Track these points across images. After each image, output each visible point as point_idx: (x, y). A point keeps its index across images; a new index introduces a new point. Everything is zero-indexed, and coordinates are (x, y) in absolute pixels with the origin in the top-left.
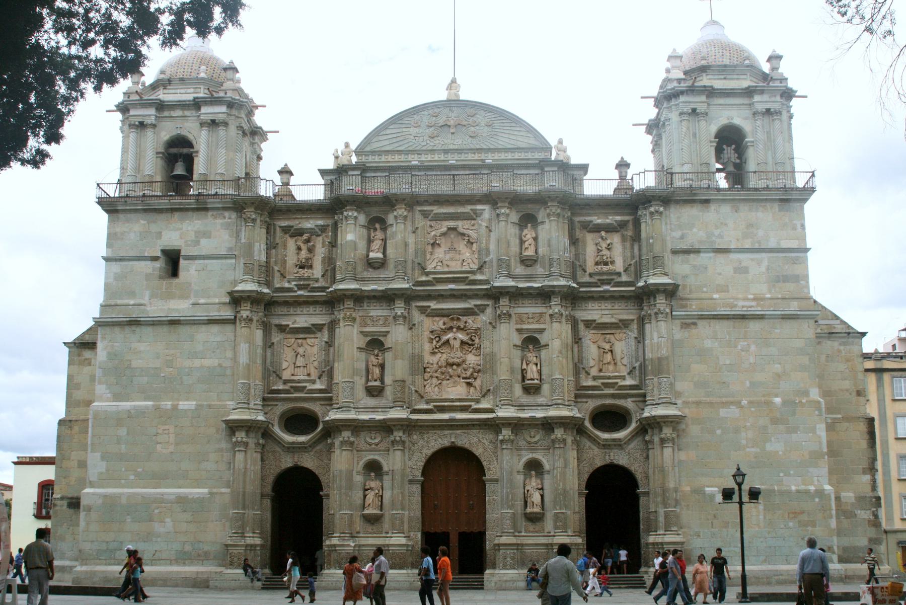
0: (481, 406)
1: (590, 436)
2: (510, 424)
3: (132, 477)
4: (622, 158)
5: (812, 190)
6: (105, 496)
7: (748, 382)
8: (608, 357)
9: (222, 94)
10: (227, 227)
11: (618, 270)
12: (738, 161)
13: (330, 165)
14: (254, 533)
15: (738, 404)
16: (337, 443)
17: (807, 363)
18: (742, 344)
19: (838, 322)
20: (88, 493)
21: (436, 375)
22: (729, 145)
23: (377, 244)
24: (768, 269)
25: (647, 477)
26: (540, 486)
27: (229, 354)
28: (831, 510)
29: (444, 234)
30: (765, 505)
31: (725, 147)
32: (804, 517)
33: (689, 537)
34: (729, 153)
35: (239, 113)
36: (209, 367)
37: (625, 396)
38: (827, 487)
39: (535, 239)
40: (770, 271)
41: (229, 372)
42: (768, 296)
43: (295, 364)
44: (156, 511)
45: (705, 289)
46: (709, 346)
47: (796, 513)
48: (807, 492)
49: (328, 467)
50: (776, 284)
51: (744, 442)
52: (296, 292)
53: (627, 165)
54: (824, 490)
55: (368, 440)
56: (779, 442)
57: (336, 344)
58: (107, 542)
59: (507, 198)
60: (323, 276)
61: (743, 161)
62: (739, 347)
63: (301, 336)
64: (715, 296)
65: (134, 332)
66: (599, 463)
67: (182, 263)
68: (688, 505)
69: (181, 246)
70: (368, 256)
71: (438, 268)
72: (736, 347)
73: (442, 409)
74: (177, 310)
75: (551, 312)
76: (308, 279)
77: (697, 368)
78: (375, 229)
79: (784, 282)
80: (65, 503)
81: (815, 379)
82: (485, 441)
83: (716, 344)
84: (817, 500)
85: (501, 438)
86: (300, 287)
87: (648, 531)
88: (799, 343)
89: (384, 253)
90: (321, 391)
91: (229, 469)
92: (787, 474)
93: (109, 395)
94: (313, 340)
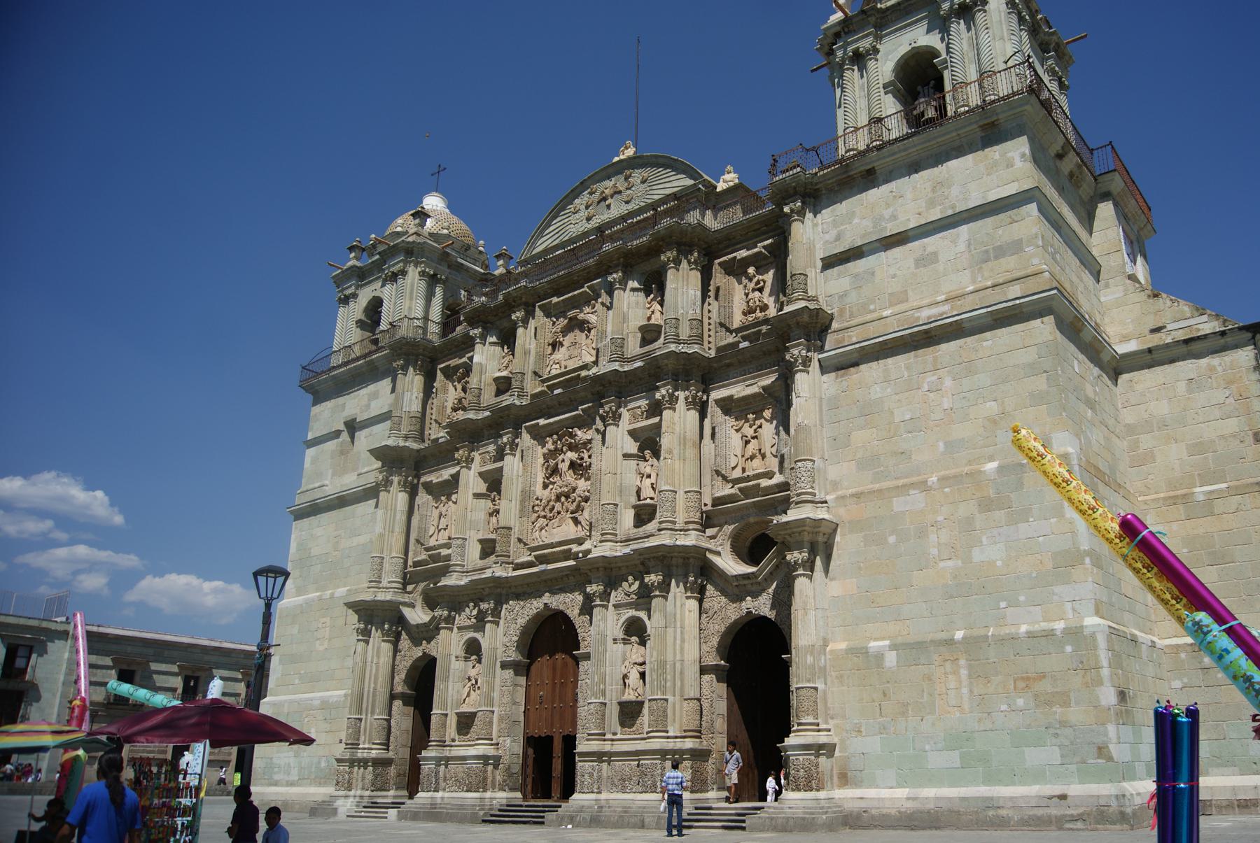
7: (941, 444)
15: (923, 486)
21: (543, 513)
24: (969, 245)
28: (1098, 667)
30: (970, 667)
32: (1046, 686)
33: (845, 734)
38: (1091, 621)
40: (972, 247)
42: (971, 288)
43: (438, 527)
45: (872, 307)
47: (1028, 679)
48: (1050, 634)
50: (983, 266)
51: (934, 551)
54: (1082, 627)
56: (995, 543)
59: (619, 259)
64: (885, 313)
68: (842, 676)
69: (356, 414)
73: (542, 560)
79: (996, 258)
81: (1061, 415)
83: (889, 390)
84: (1069, 649)
88: (1029, 356)
92: (1013, 603)
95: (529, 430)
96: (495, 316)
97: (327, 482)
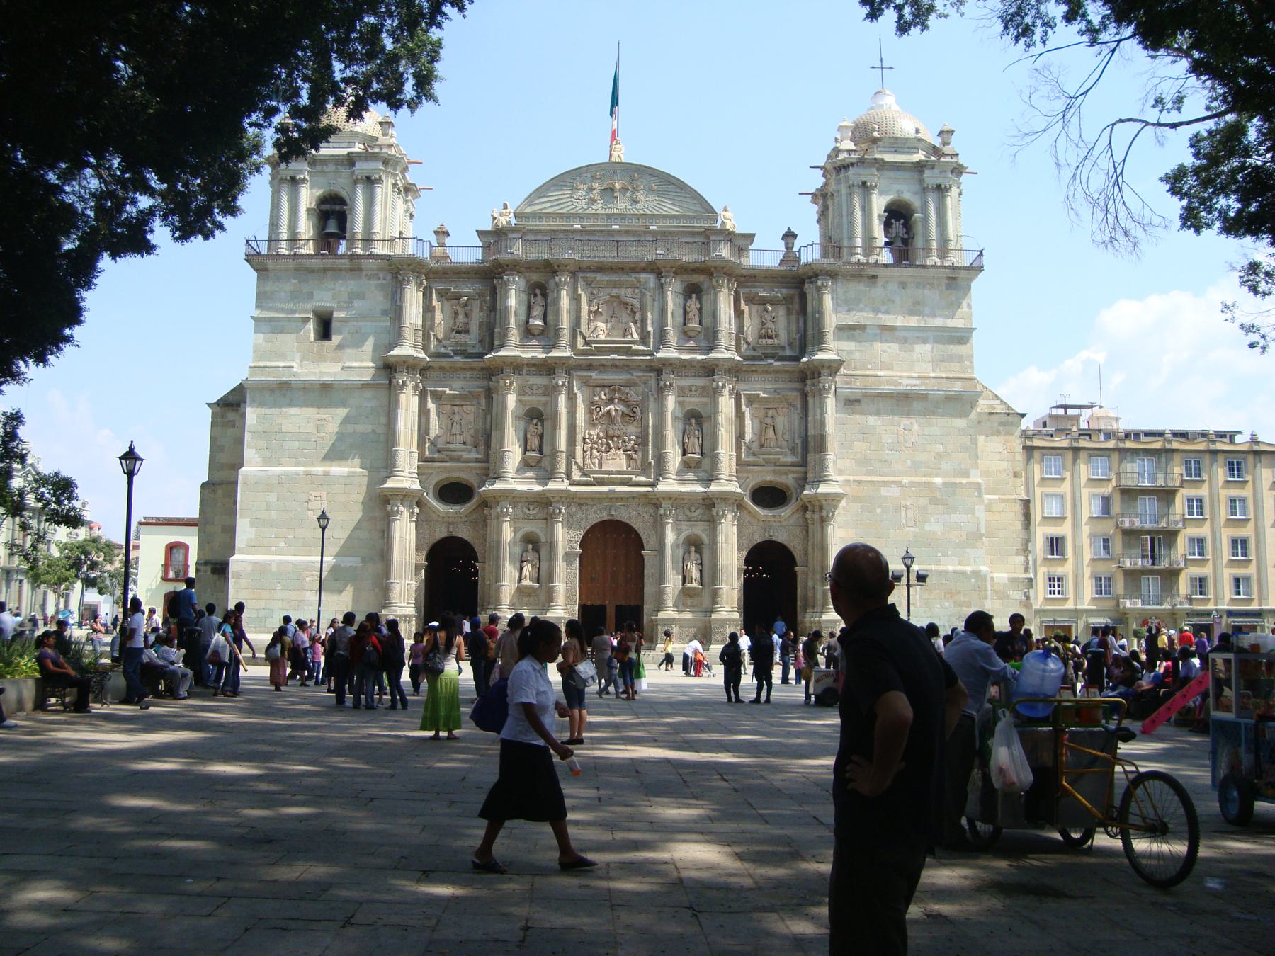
0: (642, 479)
1: (750, 512)
2: (670, 498)
3: (282, 544)
4: (789, 229)
5: (981, 269)
6: (255, 563)
7: (909, 461)
8: (771, 431)
9: (377, 150)
10: (382, 288)
11: (782, 344)
12: (906, 236)
13: (488, 227)
14: (408, 603)
16: (494, 514)
17: (969, 443)
19: (999, 402)
20: (237, 561)
22: (898, 220)
23: (537, 311)
25: (806, 554)
26: (699, 562)
27: (383, 420)
28: (986, 590)
29: (607, 302)
31: (893, 221)
34: (897, 226)
35: (395, 170)
36: (363, 433)
37: (786, 474)
39: (700, 310)
41: (382, 438)
42: (933, 375)
44: (308, 579)
45: (870, 366)
46: (873, 423)
47: (951, 593)
48: (963, 573)
49: (484, 538)
51: (904, 521)
52: (452, 357)
53: (795, 236)
55: (526, 510)
57: (494, 414)
58: (257, 610)
59: (672, 267)
60: (480, 342)
61: (911, 236)
62: (902, 426)
63: (458, 403)
65: (284, 395)
66: (758, 539)
67: (335, 325)
70: (527, 322)
71: (601, 336)
73: (600, 482)
74: (329, 374)
75: (714, 385)
76: (465, 344)
78: (535, 295)
80: (209, 568)
82: (645, 514)
84: (973, 580)
85: (662, 511)
86: (456, 353)
87: (805, 608)
89: (545, 320)
90: (477, 461)
91: (383, 537)
93: (259, 460)
94: (469, 407)
95: (580, 378)
96: (526, 268)
97: (294, 364)
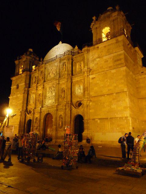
18: (106, 80)
28: (130, 124)
30: (110, 123)
72: (104, 81)
77: (96, 88)
79: (117, 61)
84: (125, 121)
88: (122, 77)
